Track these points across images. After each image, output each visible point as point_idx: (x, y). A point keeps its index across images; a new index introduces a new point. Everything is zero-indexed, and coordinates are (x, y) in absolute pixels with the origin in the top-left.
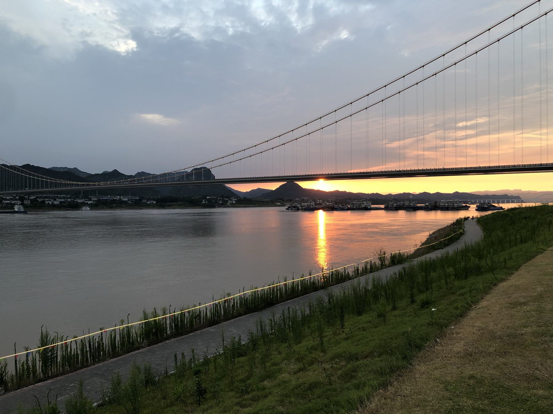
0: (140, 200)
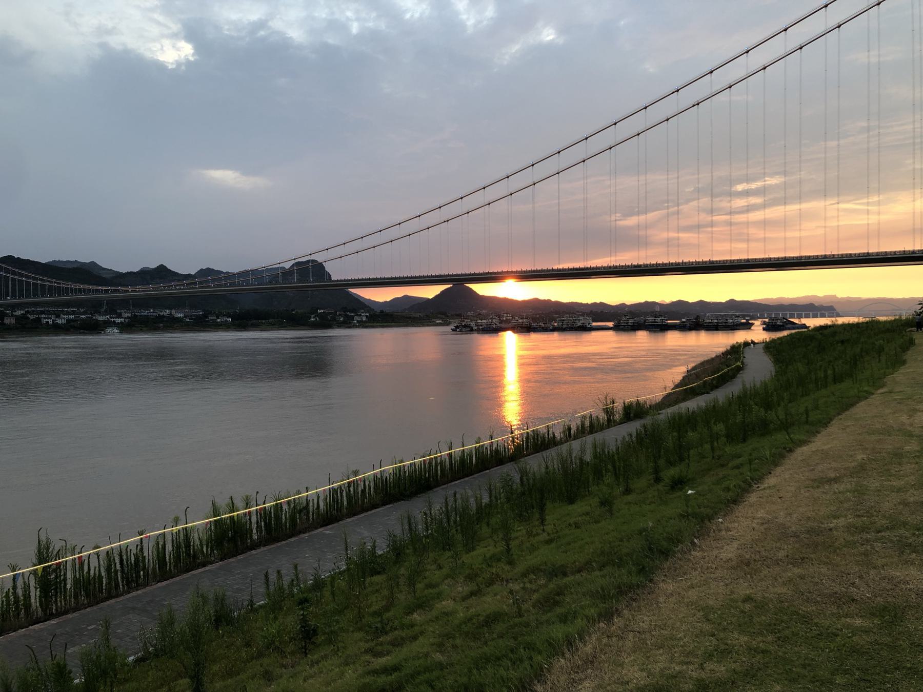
0: (205, 316)
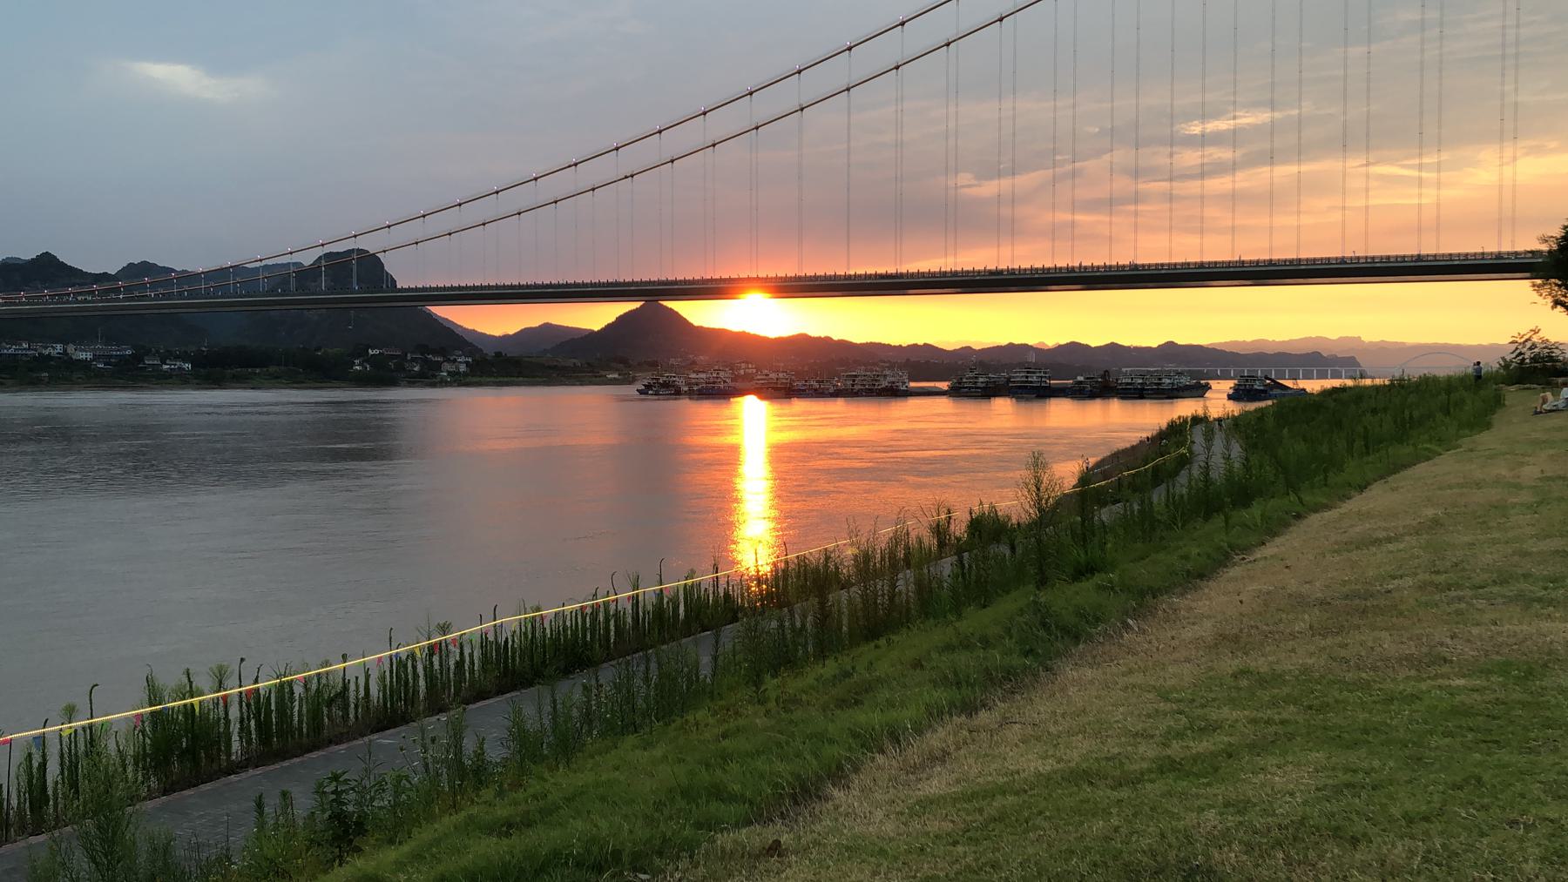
0: (137, 358)
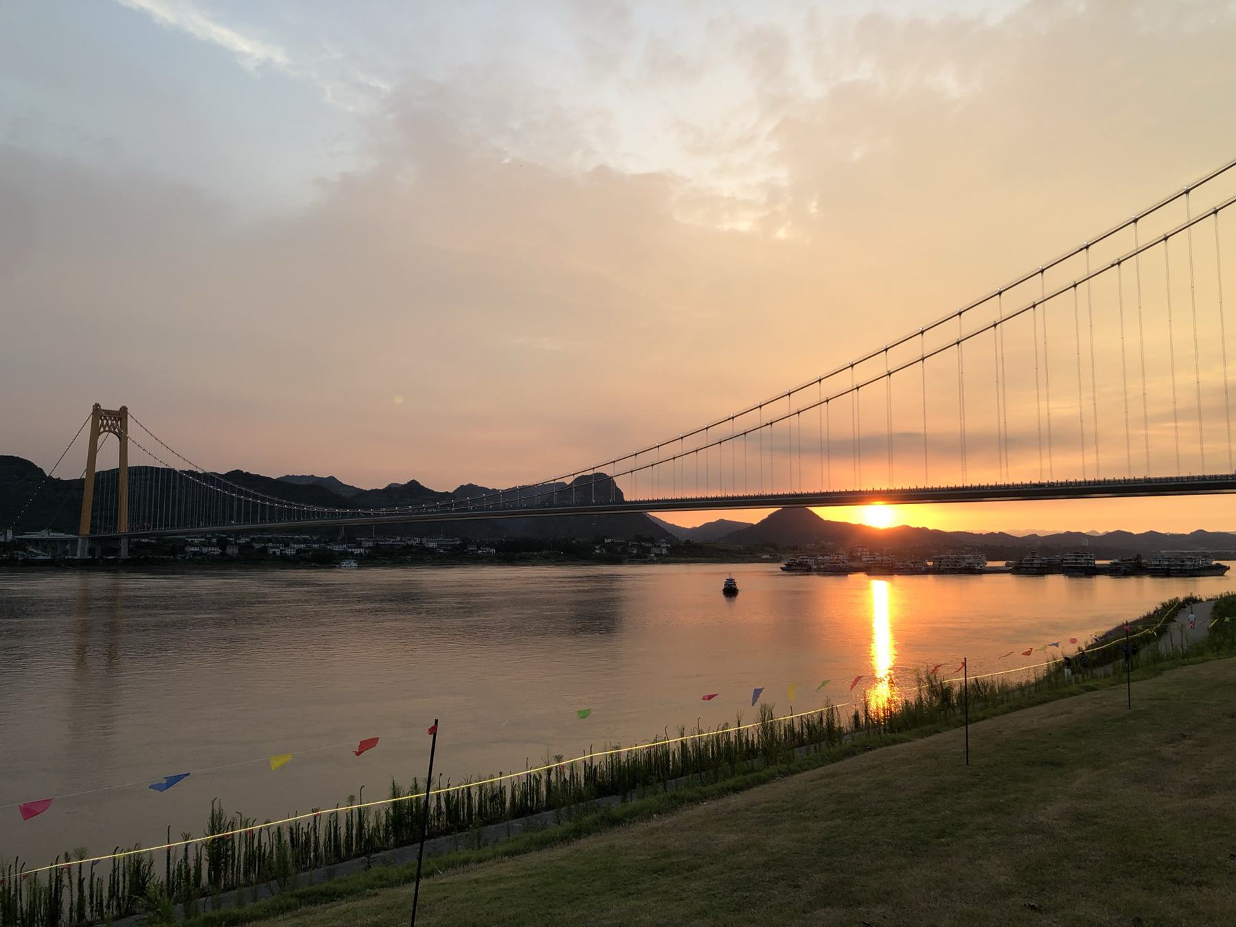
0: (463, 546)
